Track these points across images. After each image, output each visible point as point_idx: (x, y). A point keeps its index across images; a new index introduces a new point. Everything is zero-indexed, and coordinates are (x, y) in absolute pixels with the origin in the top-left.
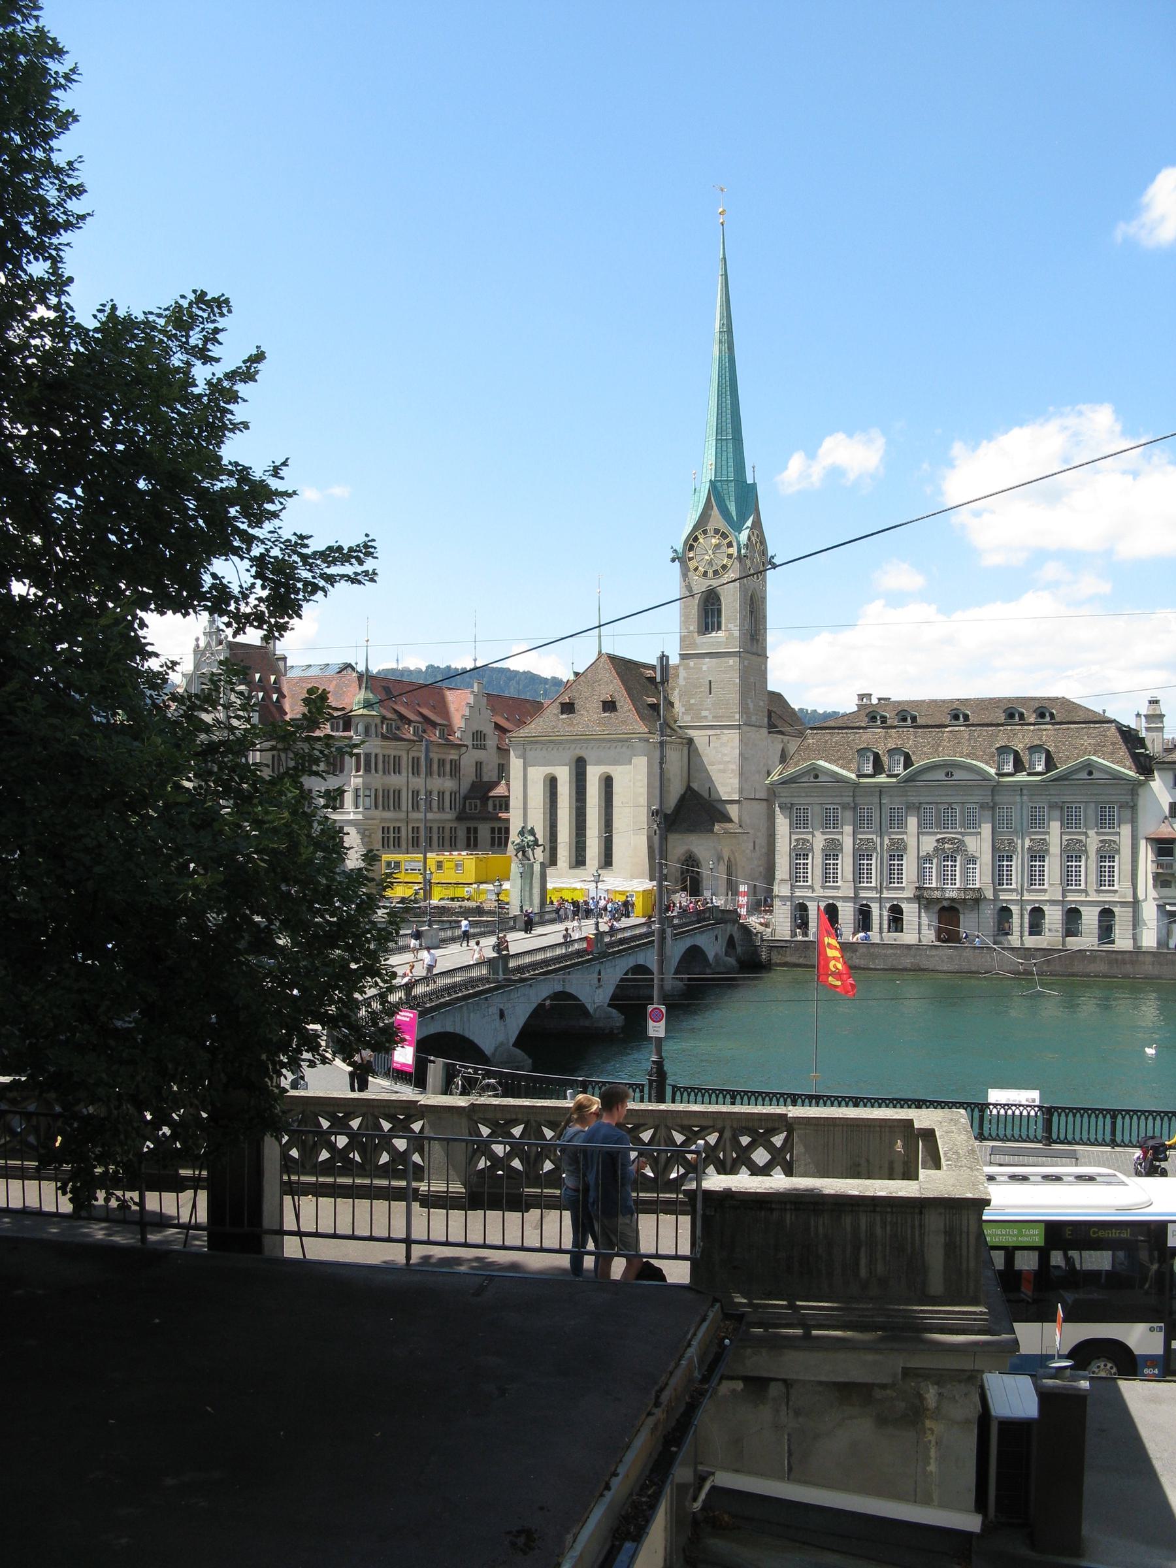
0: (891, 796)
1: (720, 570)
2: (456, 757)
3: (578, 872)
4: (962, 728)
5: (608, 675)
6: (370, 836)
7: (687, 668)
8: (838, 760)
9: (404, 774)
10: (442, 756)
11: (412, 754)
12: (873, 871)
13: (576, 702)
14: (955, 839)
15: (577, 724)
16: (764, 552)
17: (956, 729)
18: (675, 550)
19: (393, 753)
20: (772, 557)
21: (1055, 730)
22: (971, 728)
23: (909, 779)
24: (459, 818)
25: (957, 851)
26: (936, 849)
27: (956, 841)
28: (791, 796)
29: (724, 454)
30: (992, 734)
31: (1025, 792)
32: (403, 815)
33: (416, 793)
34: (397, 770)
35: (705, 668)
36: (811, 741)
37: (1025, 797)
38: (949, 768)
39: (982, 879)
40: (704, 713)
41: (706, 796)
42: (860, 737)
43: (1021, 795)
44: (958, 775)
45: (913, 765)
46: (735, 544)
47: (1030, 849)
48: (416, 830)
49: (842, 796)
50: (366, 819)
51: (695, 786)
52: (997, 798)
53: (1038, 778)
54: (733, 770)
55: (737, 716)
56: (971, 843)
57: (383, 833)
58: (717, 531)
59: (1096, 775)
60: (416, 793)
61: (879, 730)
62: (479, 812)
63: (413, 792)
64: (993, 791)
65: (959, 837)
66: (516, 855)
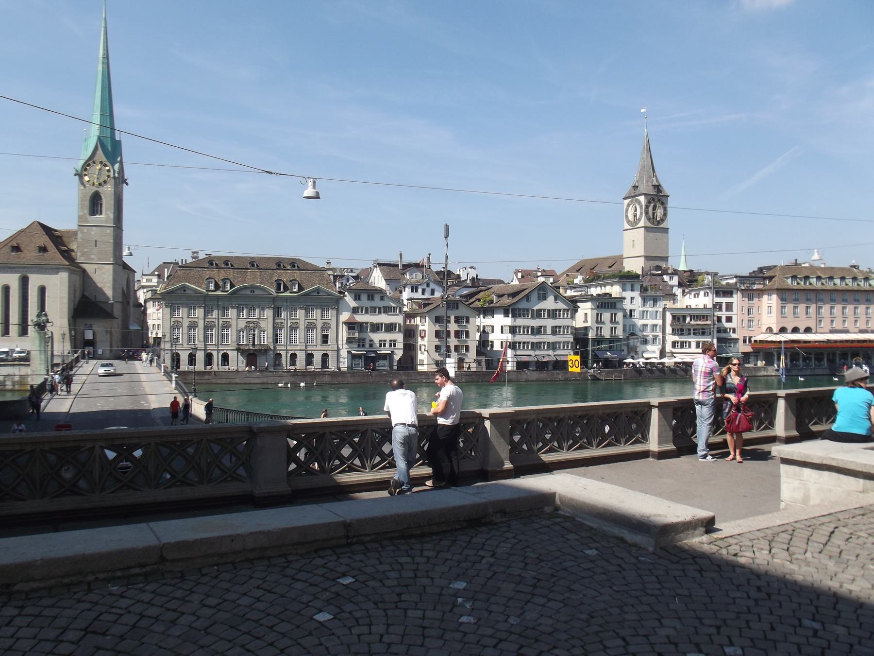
1: (103, 184)
7: (82, 232)
13: (21, 246)
15: (23, 258)
17: (254, 270)
18: (77, 170)
20: (126, 179)
26: (246, 326)
35: (93, 233)
38: (252, 288)
39: (267, 340)
40: (92, 257)
41: (93, 300)
43: (287, 302)
47: (290, 326)
51: (86, 294)
53: (296, 295)
54: (109, 287)
55: (112, 259)
56: (263, 324)
59: (321, 294)
64: (273, 300)
65: (257, 320)
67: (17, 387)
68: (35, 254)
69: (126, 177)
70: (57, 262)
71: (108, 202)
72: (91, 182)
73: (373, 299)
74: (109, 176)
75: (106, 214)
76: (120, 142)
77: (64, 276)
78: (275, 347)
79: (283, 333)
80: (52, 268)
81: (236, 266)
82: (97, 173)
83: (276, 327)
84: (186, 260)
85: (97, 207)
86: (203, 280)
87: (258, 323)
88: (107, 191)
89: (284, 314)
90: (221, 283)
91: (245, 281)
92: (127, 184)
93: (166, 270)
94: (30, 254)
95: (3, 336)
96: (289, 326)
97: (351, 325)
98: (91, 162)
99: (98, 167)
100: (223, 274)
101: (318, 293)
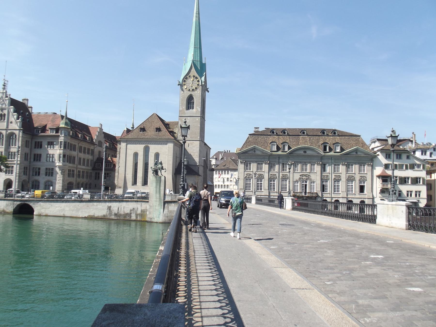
0: (283, 159)
2: (93, 148)
3: (145, 187)
4: (306, 137)
5: (156, 120)
6: (64, 172)
8: (262, 146)
9: (77, 151)
10: (89, 147)
11: (80, 145)
12: (276, 186)
13: (145, 128)
14: (307, 175)
16: (206, 86)
17: (304, 137)
18: (179, 82)
19: (73, 143)
21: (340, 138)
22: (309, 137)
23: (291, 153)
24: (93, 169)
25: (308, 179)
26: (300, 179)
27: (308, 176)
28: (245, 158)
29: (197, 52)
30: (317, 139)
31: (333, 159)
32: (75, 166)
33: (80, 159)
34: (75, 150)
36: (250, 139)
37: (333, 161)
38: (305, 149)
39: (317, 189)
42: (269, 138)
43: (331, 160)
44: (309, 152)
45: (291, 149)
46: (200, 81)
47: (334, 179)
48: (79, 172)
49: (264, 159)
50: (64, 166)
52: (322, 160)
53: (339, 154)
54: (197, 155)
55: (199, 137)
56: (313, 177)
57: (69, 171)
58: (194, 76)
59: (359, 153)
60: (80, 159)
61: (276, 136)
62: (100, 168)
63: (79, 158)
64: (321, 158)
65: (308, 174)
66: (153, 173)
67: (139, 218)
68: (153, 133)
69: (208, 87)
70: (167, 137)
71: (197, 101)
72: (188, 89)
73: (400, 158)
74: (198, 85)
75: (196, 109)
76: (205, 64)
77: (171, 146)
78: (322, 195)
79: (329, 184)
80: (163, 141)
81: (290, 134)
82: (191, 83)
83: (323, 180)
84: (230, 151)
85: (191, 104)
86: (267, 144)
87: (309, 175)
88: (197, 95)
89: (329, 169)
90: (281, 146)
91: (298, 145)
92: (208, 92)
93: (220, 155)
94: (151, 133)
95: (133, 185)
96: (333, 178)
97: (385, 178)
98: (188, 76)
99: (192, 79)
100: (281, 139)
101: (356, 153)
